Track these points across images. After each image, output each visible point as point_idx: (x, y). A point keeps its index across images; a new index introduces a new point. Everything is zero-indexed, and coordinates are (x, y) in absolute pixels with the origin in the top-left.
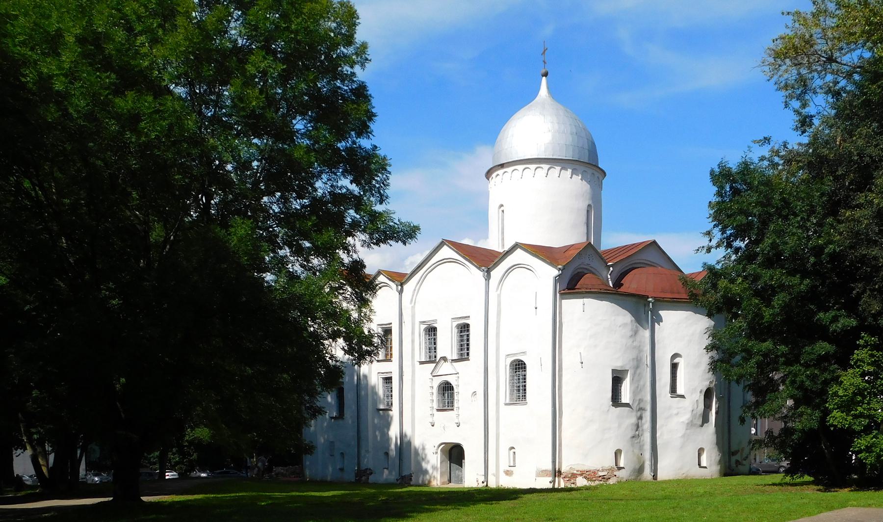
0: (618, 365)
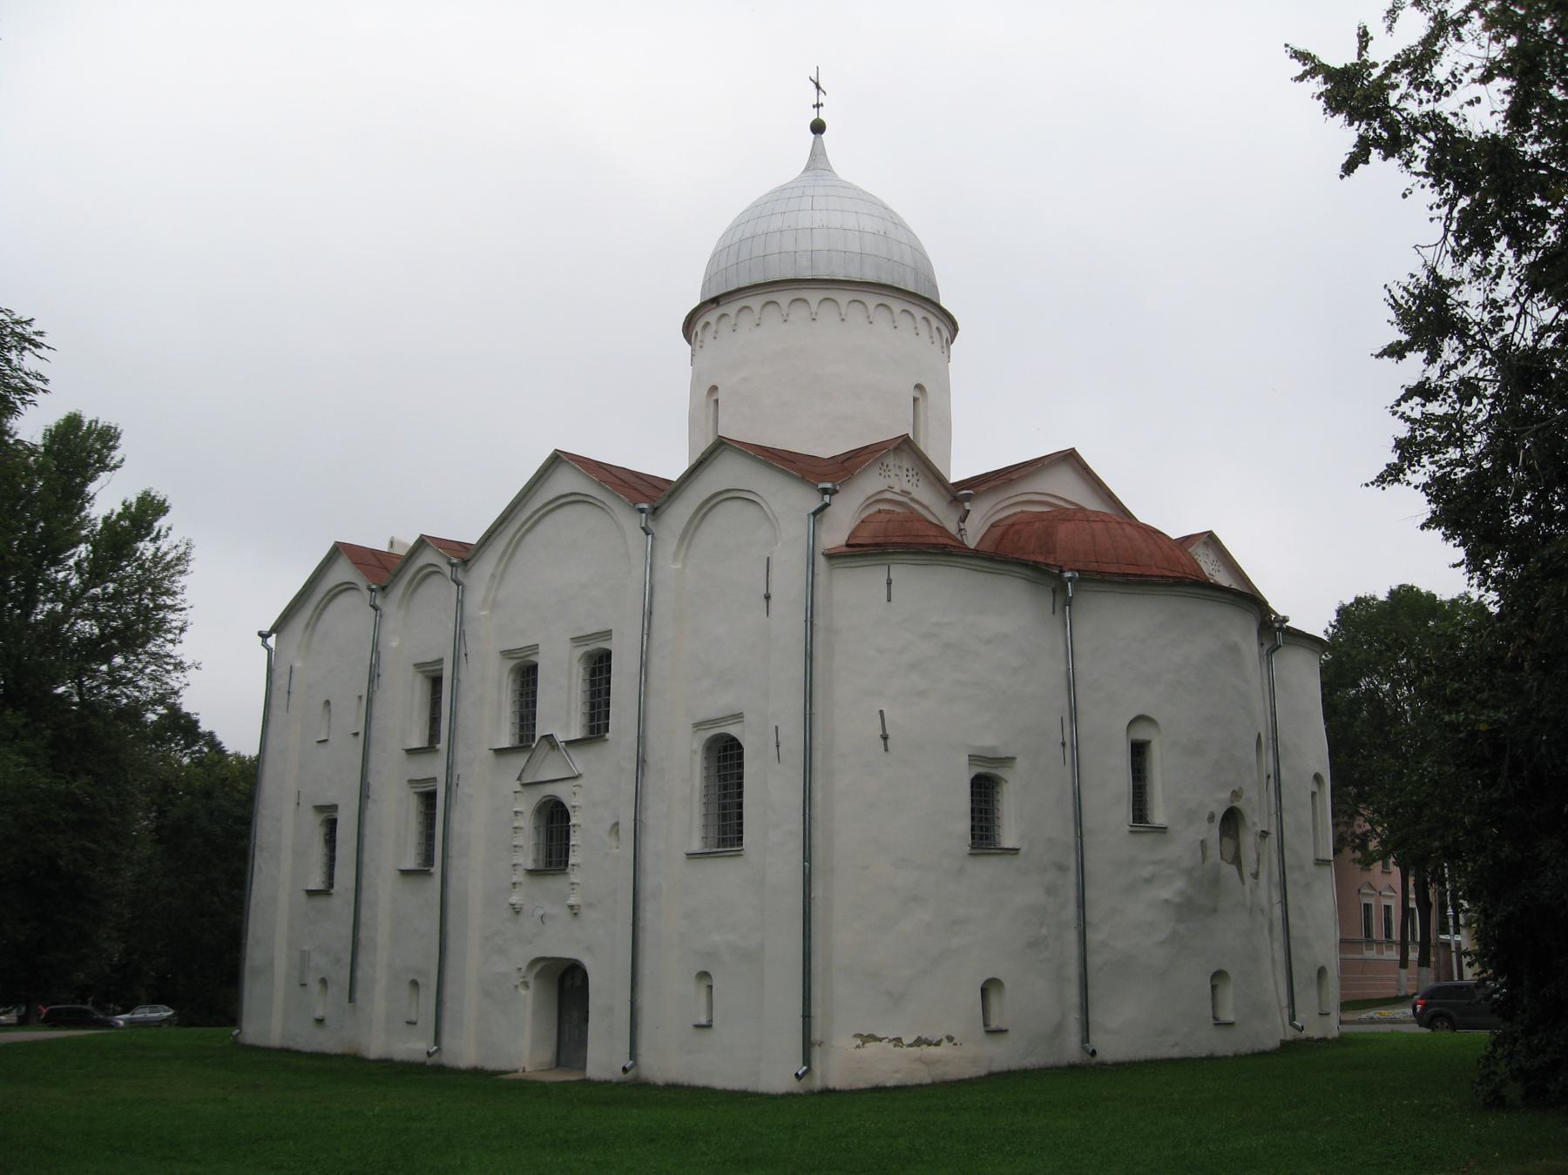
0: (989, 741)
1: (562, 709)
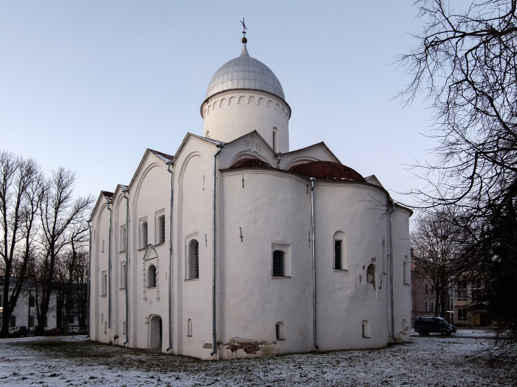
0: (279, 239)
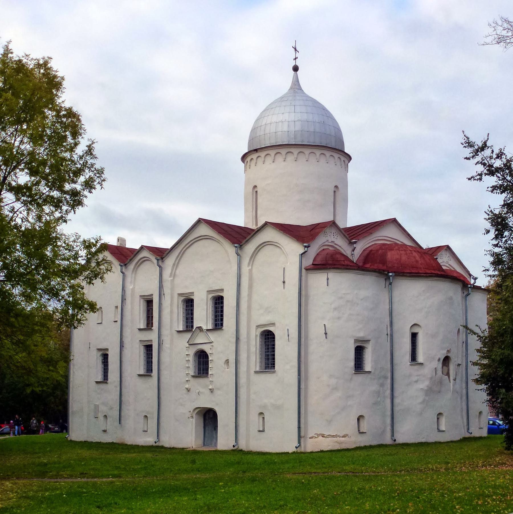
0: (361, 335)
1: (203, 316)
